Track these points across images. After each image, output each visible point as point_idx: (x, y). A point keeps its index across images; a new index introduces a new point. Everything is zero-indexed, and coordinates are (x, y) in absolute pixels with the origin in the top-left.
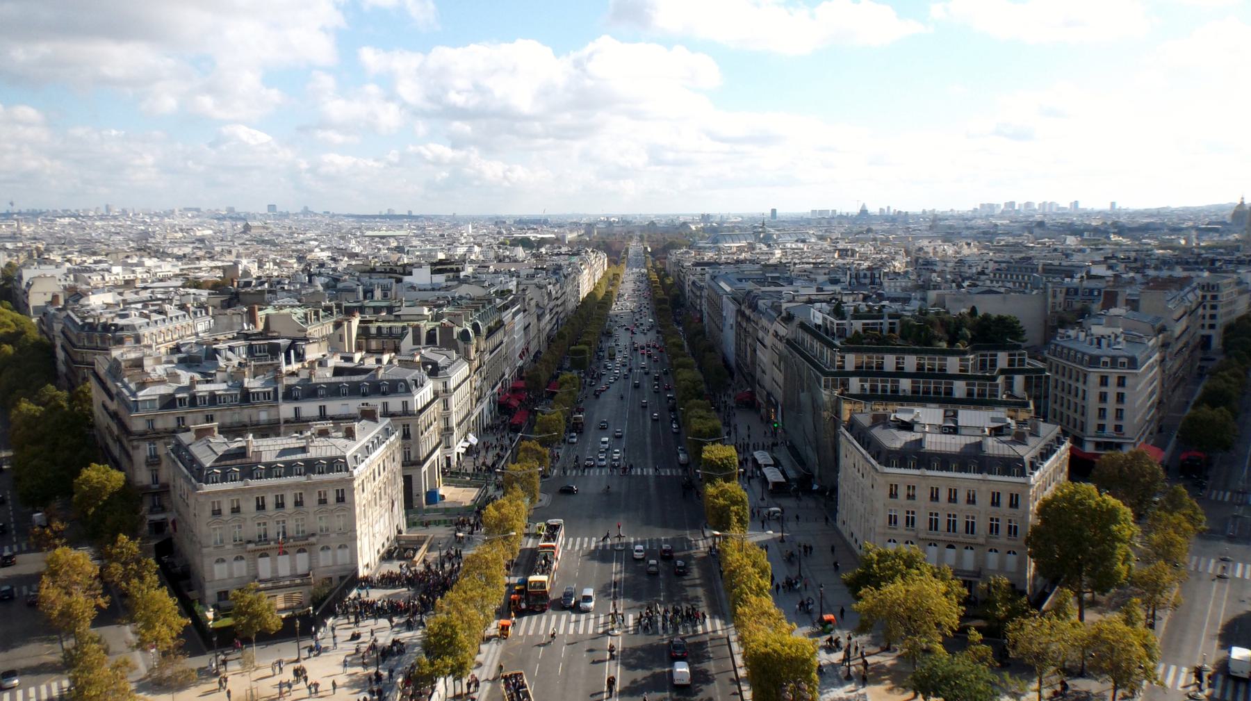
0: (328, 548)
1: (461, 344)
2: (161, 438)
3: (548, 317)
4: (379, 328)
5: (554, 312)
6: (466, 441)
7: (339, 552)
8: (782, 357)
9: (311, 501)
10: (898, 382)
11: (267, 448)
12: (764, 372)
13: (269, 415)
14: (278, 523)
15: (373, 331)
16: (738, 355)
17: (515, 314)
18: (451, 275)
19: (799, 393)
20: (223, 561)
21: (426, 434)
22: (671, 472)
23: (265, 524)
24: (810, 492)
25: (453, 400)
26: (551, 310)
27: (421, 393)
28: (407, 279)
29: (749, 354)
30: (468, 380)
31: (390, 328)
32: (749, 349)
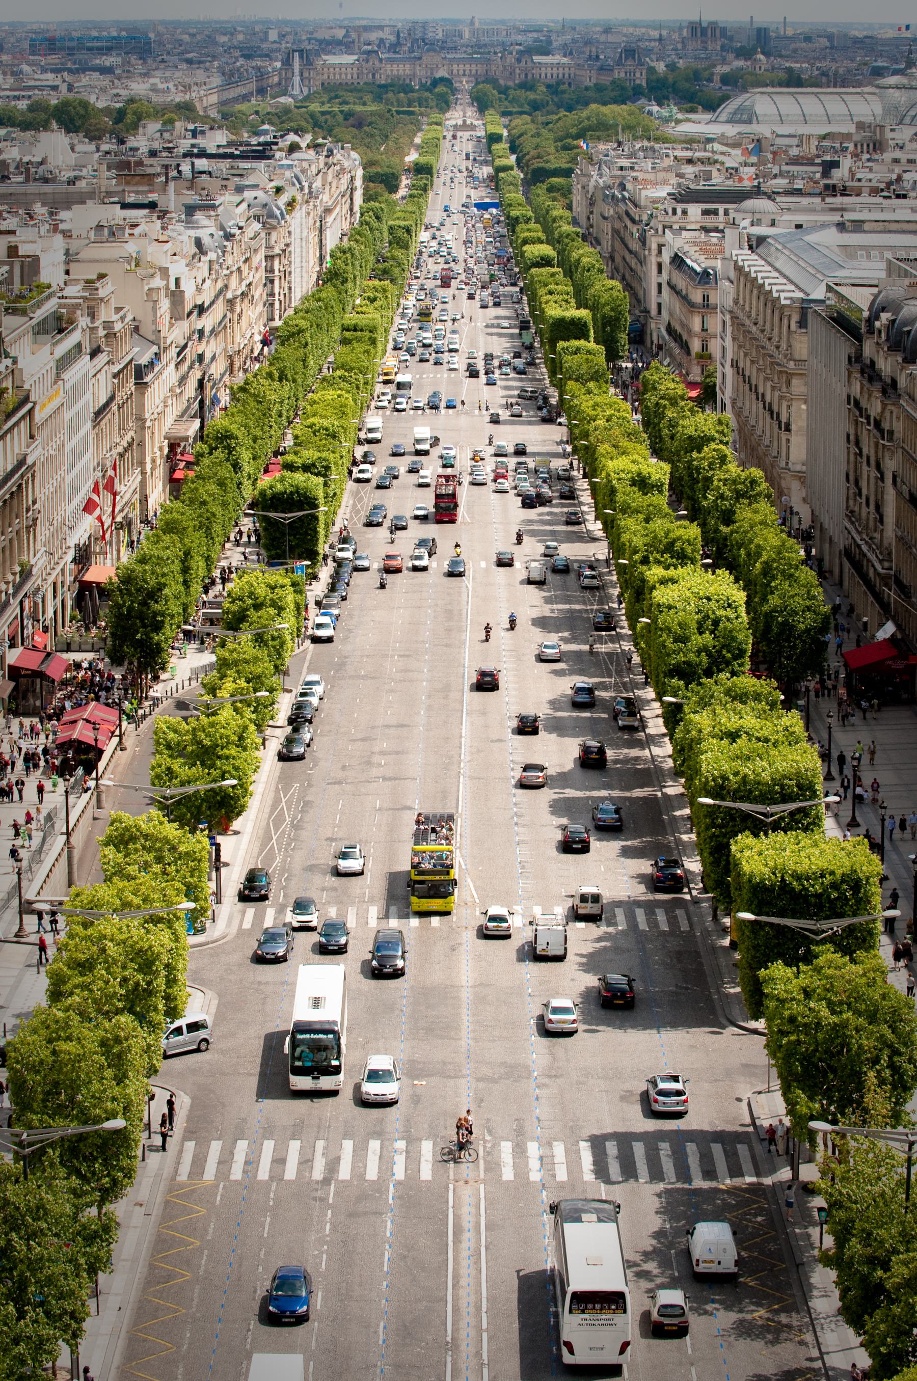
16: (851, 515)
17: (63, 364)
32: (890, 495)
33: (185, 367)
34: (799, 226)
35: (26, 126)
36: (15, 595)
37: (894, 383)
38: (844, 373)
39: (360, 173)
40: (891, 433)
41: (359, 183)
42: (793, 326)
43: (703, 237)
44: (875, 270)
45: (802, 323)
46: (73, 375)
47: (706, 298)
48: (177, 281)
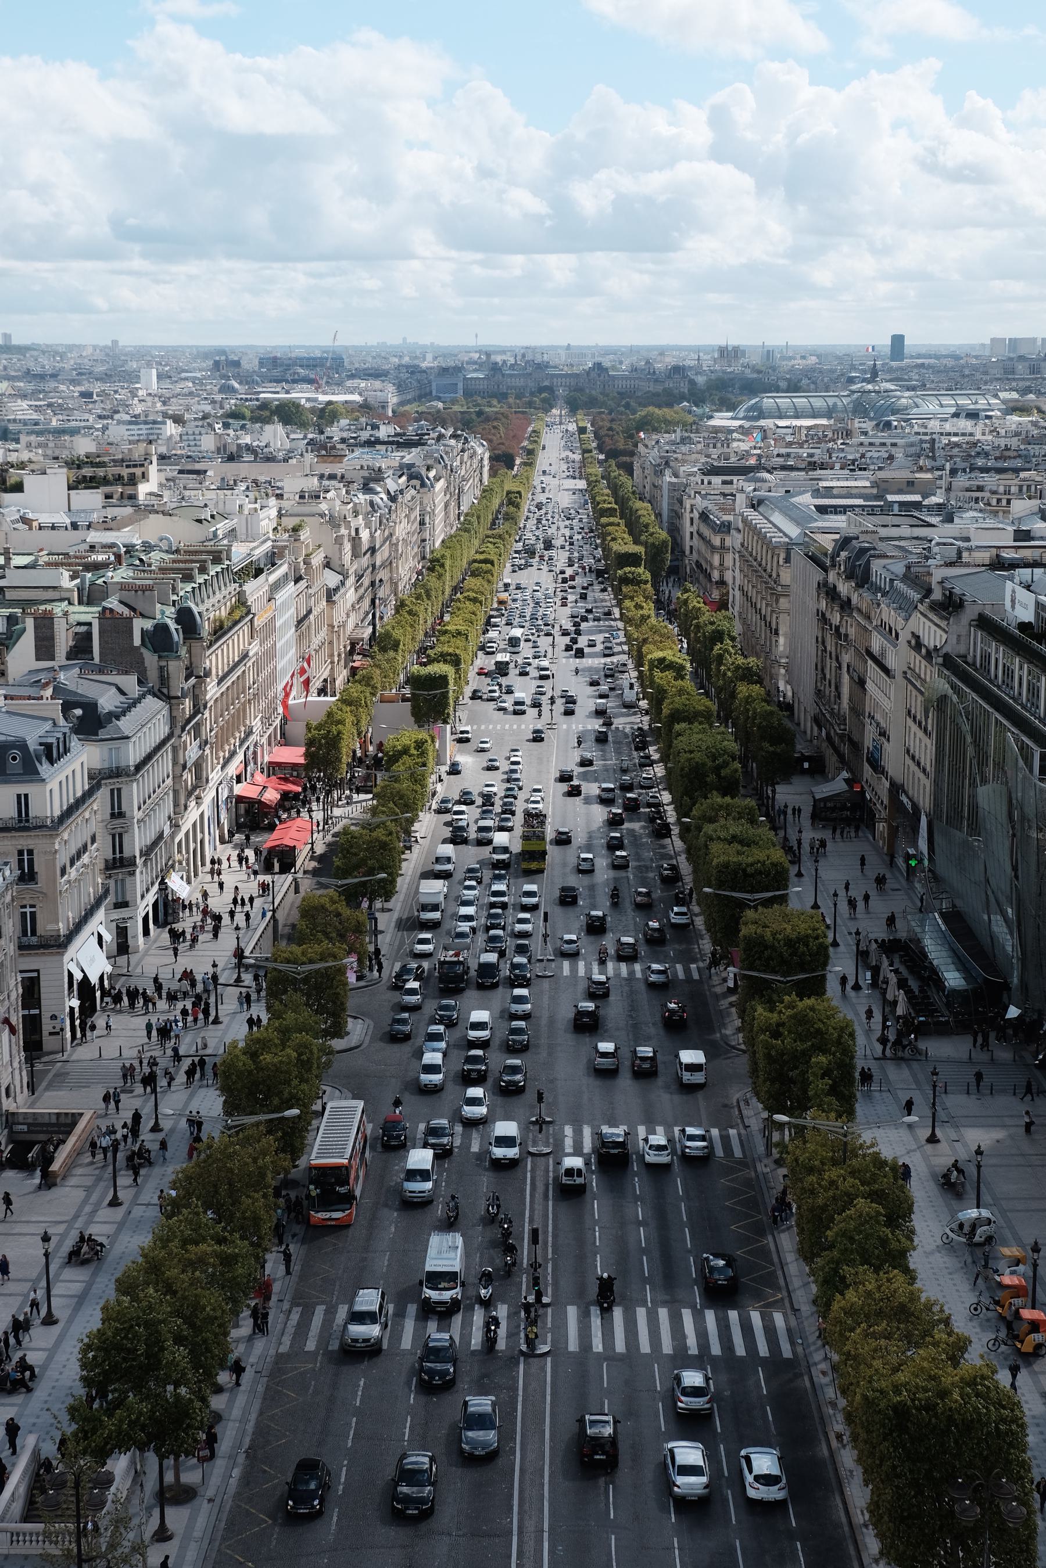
1: (150, 659)
12: (883, 734)
16: (819, 693)
17: (276, 587)
21: (73, 873)
27: (62, 777)
29: (845, 690)
32: (846, 679)
33: (362, 590)
34: (787, 492)
35: (254, 420)
36: (240, 746)
37: (849, 600)
38: (815, 593)
39: (487, 455)
40: (846, 635)
41: (486, 462)
42: (781, 562)
45: (787, 560)
46: (282, 596)
47: (723, 541)
48: (357, 530)
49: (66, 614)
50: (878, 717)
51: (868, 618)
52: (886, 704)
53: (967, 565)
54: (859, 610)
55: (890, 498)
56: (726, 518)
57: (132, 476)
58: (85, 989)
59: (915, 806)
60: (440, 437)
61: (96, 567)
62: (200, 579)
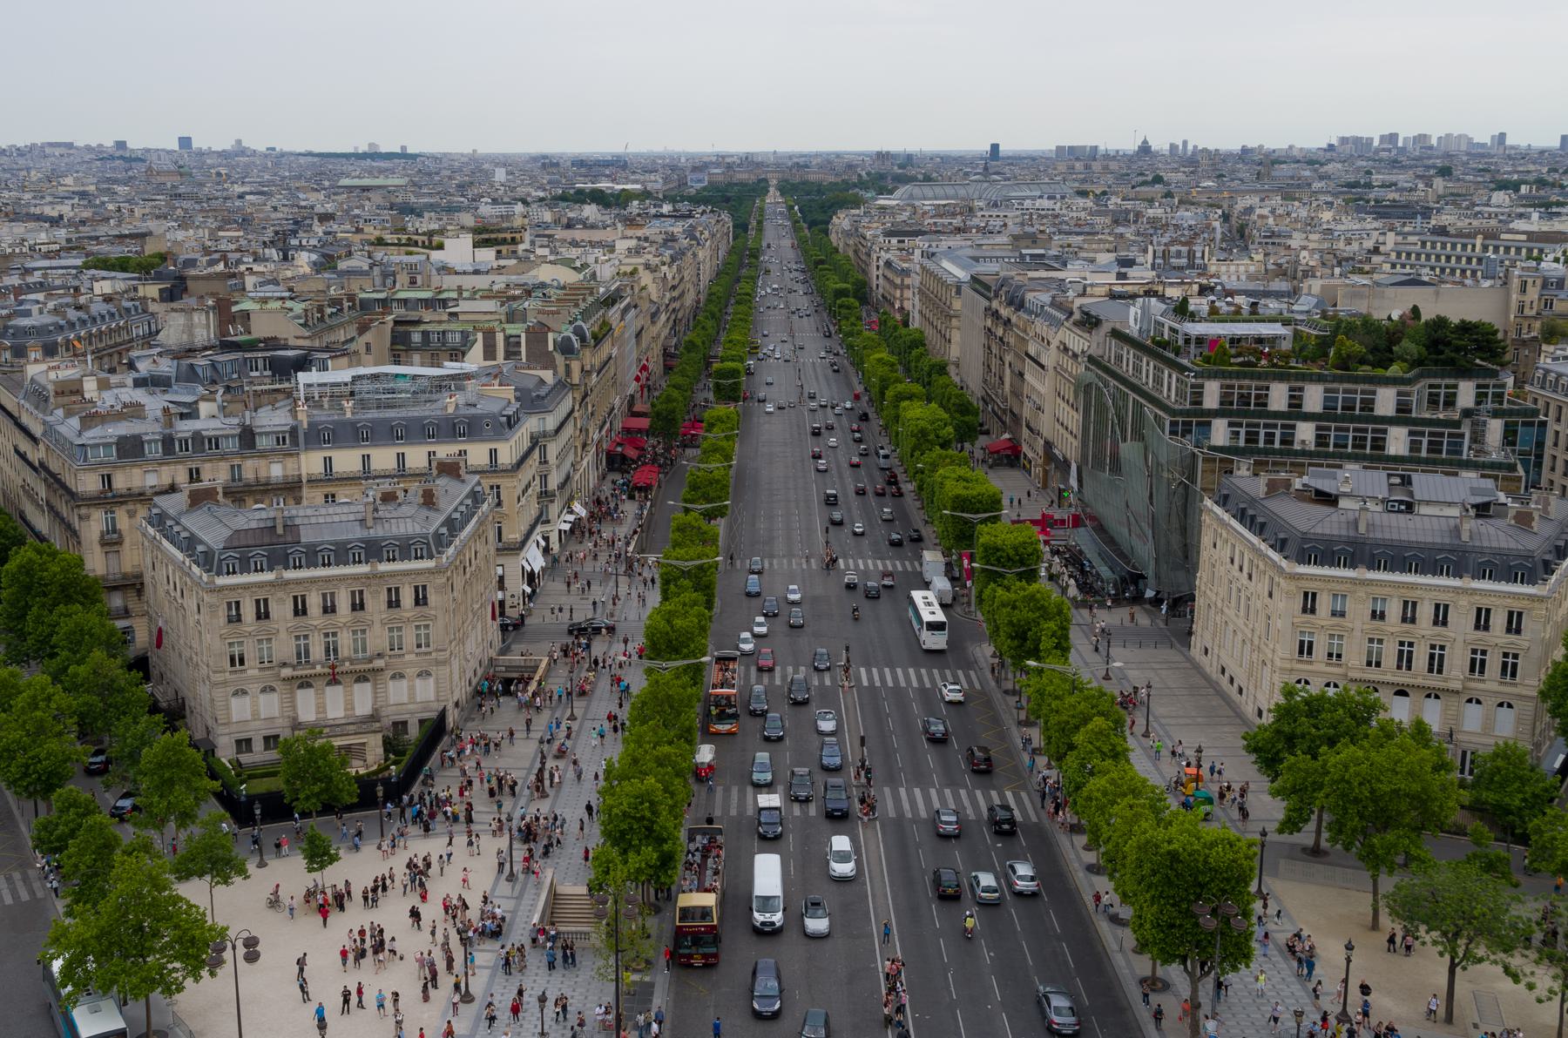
0: (402, 676)
1: (560, 360)
2: (122, 503)
3: (663, 317)
4: (425, 334)
5: (671, 308)
6: (571, 512)
7: (418, 682)
8: (1084, 389)
9: (376, 603)
10: (1293, 427)
11: (306, 521)
13: (284, 468)
14: (327, 635)
15: (416, 338)
16: (985, 381)
17: (625, 311)
18: (504, 248)
19: (1115, 445)
20: (244, 692)
21: (523, 500)
22: (903, 565)
23: (306, 637)
24: (1138, 599)
25: (553, 449)
26: (667, 306)
27: (516, 438)
28: (436, 255)
29: (1007, 380)
30: (572, 420)
31: (444, 332)
32: (1008, 371)
35: (576, 202)
37: (1009, 320)
39: (731, 224)
43: (898, 253)
44: (992, 267)
47: (902, 280)
49: (503, 330)
50: (1034, 397)
51: (1025, 331)
52: (1042, 390)
53: (1092, 296)
54: (1018, 327)
55: (1024, 251)
56: (905, 265)
57: (513, 239)
58: (531, 578)
59: (1064, 457)
60: (704, 212)
61: (514, 298)
62: (583, 306)
